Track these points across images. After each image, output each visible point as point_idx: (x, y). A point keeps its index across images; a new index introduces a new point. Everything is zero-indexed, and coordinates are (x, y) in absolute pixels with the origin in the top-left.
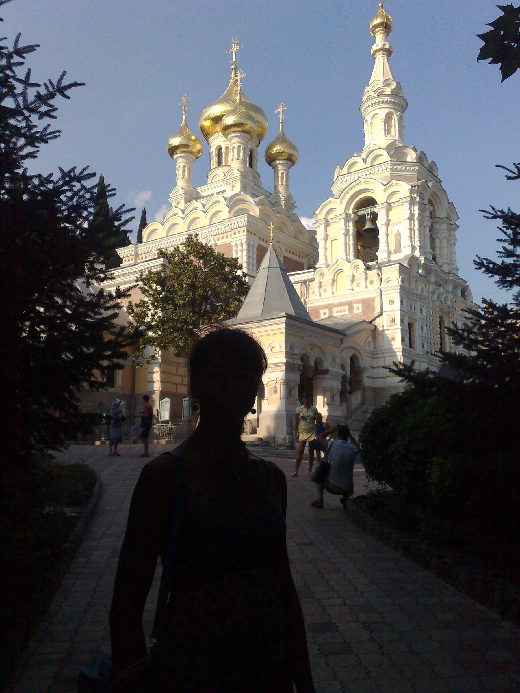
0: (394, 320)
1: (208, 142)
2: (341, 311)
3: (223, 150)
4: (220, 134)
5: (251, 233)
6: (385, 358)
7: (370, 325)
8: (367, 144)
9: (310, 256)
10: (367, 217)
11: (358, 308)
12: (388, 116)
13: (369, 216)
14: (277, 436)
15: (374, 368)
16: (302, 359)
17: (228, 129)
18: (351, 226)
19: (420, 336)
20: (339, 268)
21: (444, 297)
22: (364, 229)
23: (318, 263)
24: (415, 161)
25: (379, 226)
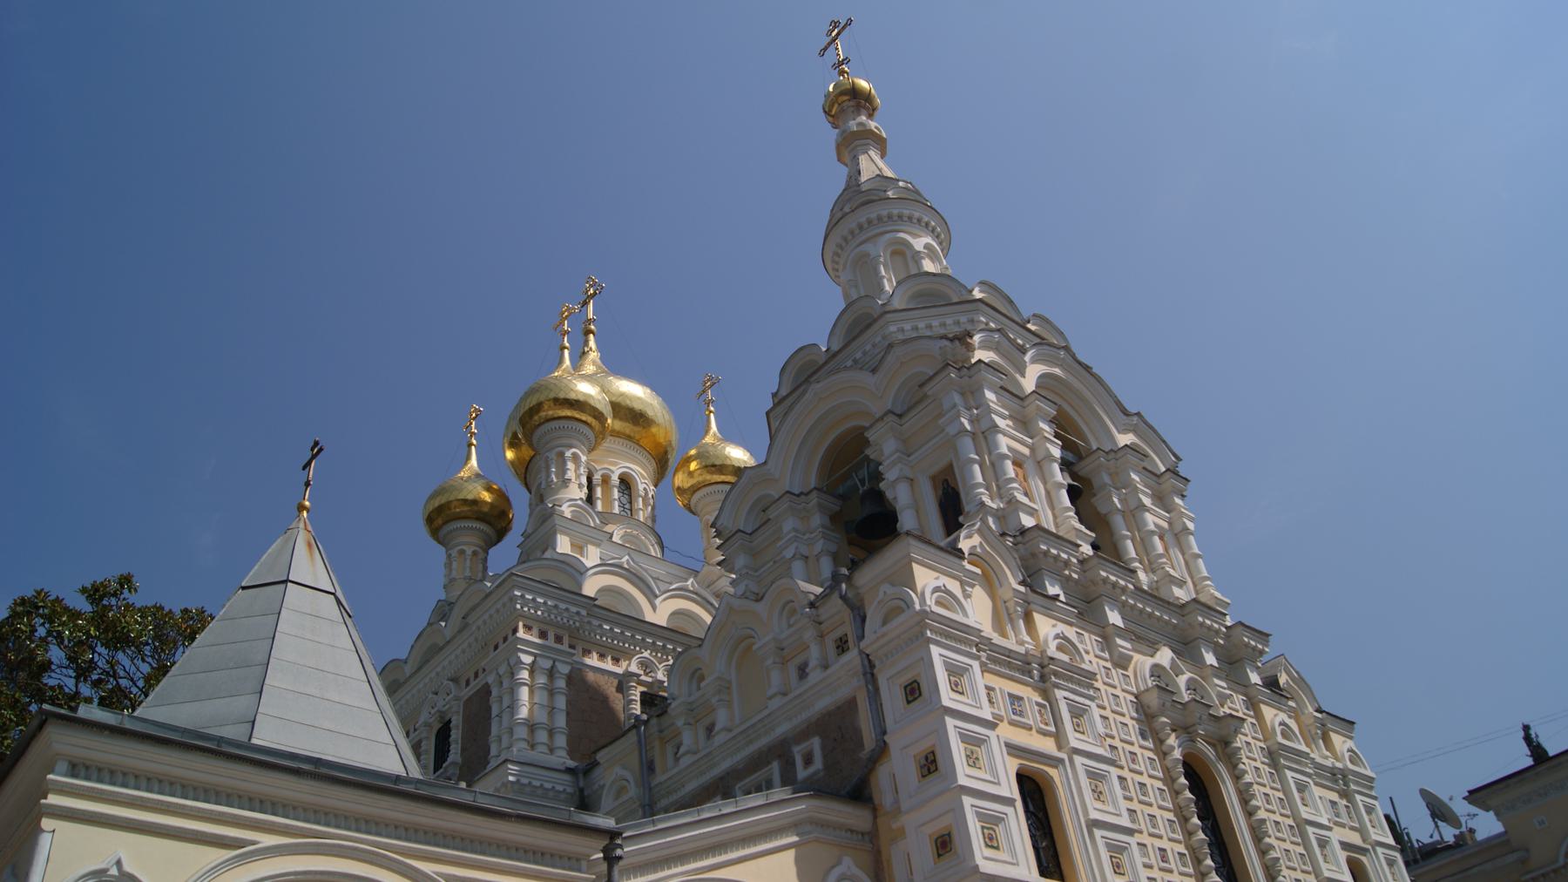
0: (934, 761)
11: (808, 761)
21: (1182, 681)
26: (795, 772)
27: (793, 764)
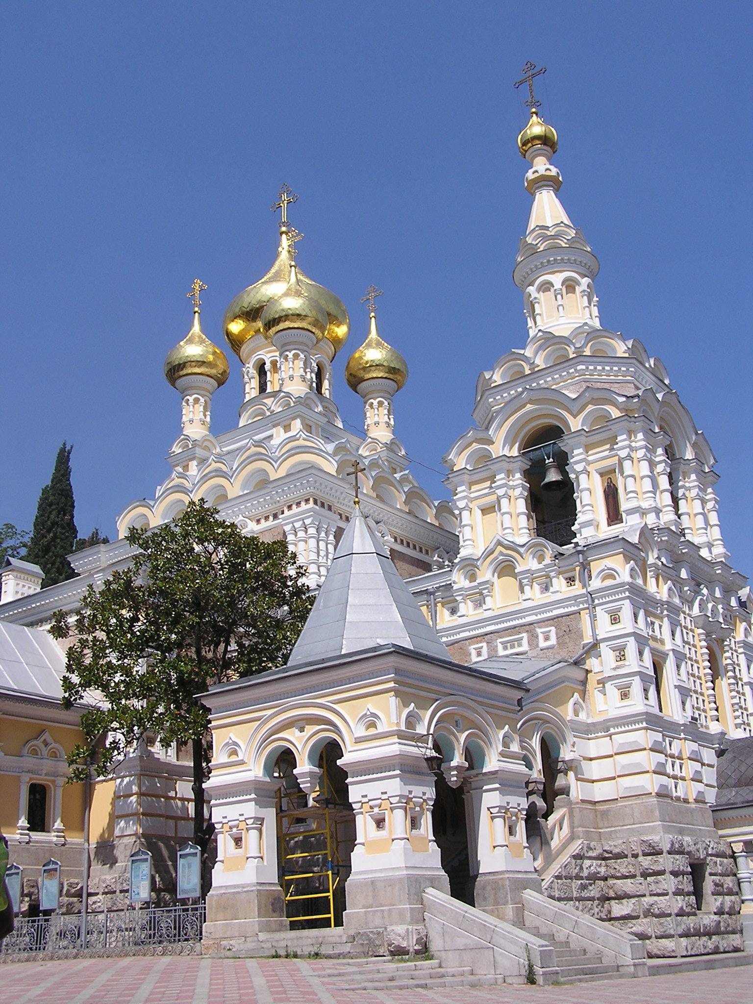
1: (240, 357)
2: (512, 647)
3: (268, 366)
4: (261, 339)
5: (323, 505)
6: (613, 736)
7: (574, 668)
8: (532, 333)
9: (441, 549)
10: (547, 461)
11: (547, 638)
12: (567, 283)
13: (551, 460)
14: (389, 928)
15: (591, 759)
16: (437, 747)
17: (273, 326)
18: (518, 479)
19: (676, 687)
20: (501, 557)
21: (710, 606)
22: (544, 482)
23: (458, 556)
24: (627, 355)
25: (572, 476)
26: (538, 641)
27: (537, 637)
